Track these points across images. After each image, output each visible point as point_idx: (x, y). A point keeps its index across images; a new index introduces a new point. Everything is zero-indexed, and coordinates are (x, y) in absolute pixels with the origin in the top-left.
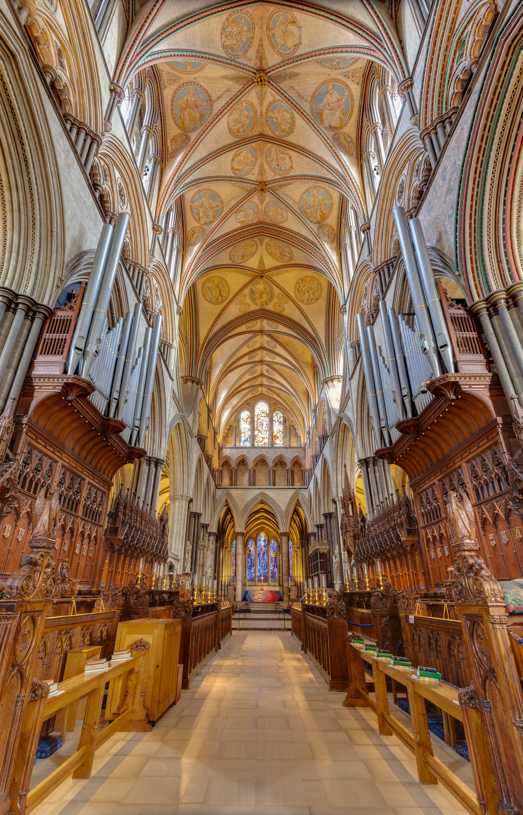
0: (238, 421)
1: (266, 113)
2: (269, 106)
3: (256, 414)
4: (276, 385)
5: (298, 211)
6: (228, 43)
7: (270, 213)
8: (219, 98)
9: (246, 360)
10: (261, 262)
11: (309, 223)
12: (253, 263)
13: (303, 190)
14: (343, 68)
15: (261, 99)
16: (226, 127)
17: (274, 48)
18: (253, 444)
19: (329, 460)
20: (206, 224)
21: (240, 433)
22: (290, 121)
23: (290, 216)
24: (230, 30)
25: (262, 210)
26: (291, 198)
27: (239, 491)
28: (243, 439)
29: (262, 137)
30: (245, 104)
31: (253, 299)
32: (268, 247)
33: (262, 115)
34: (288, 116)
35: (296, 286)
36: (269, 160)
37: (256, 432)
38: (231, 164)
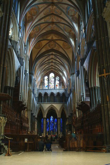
0: (44, 80)
3: (50, 77)
4: (57, 69)
8: (41, 8)
9: (47, 62)
10: (52, 38)
12: (50, 38)
18: (48, 88)
19: (72, 99)
20: (36, 32)
21: (44, 84)
23: (61, 30)
27: (44, 104)
28: (45, 86)
29: (53, 14)
31: (49, 46)
35: (63, 44)
37: (50, 84)
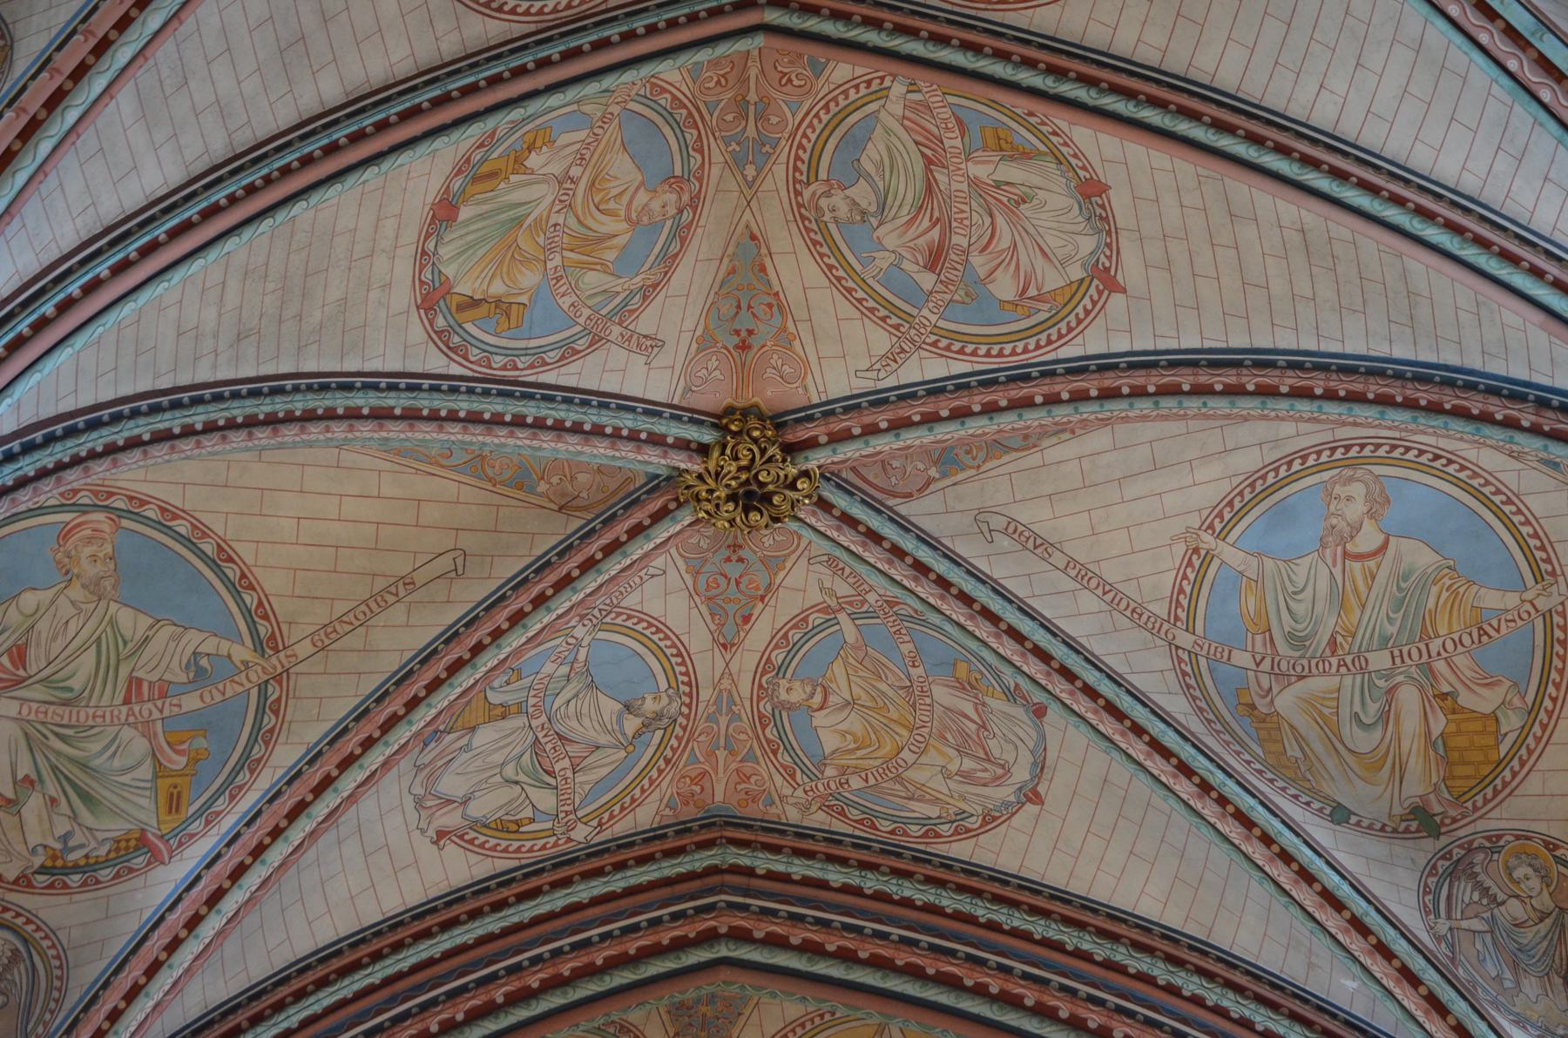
5: (1177, 706)
11: (1322, 832)
26: (1083, 575)
36: (838, 199)
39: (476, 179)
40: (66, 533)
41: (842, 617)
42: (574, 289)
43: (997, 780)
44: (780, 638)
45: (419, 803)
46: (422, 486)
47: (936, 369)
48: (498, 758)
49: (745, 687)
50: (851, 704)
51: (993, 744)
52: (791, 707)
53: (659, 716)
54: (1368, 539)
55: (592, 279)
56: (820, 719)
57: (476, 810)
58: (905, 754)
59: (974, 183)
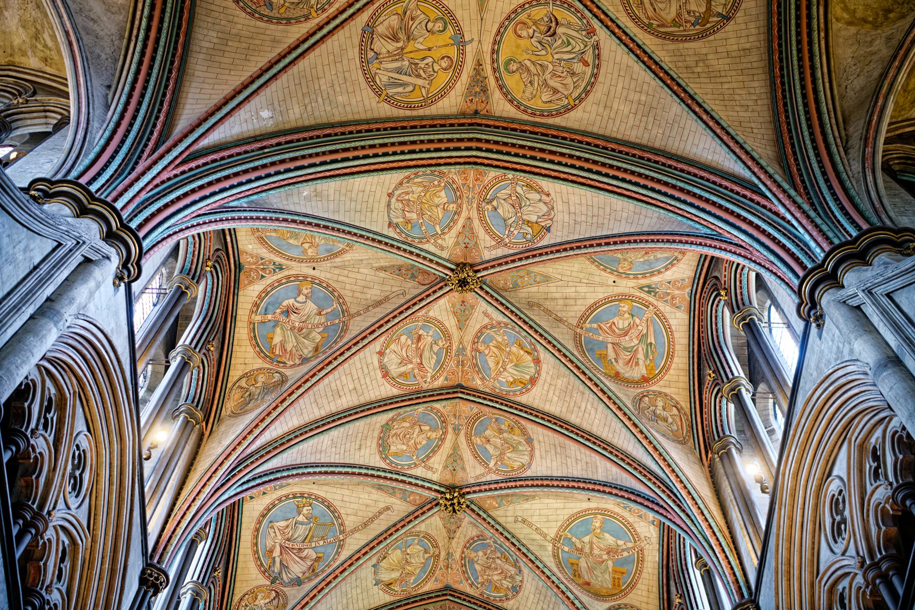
1: (445, 433)
2: (439, 447)
6: (513, 571)
7: (443, 197)
13: (347, 257)
14: (287, 497)
15: (455, 456)
16: (537, 453)
17: (427, 536)
22: (391, 440)
24: (504, 582)
25: (470, 202)
30: (492, 464)
32: (453, 52)
33: (454, 429)
34: (396, 446)
36: (441, 344)
38: (538, 372)
39: (525, 384)
40: (630, 269)
41: (440, 232)
42: (504, 340)
43: (399, 196)
44: (455, 222)
45: (553, 208)
46: (543, 270)
47: (420, 314)
48: (530, 208)
49: (465, 206)
50: (437, 206)
51: (401, 206)
52: (453, 202)
53: (487, 203)
54: (306, 246)
55: (500, 340)
56: (445, 200)
57: (537, 196)
58: (423, 194)
59: (411, 363)
